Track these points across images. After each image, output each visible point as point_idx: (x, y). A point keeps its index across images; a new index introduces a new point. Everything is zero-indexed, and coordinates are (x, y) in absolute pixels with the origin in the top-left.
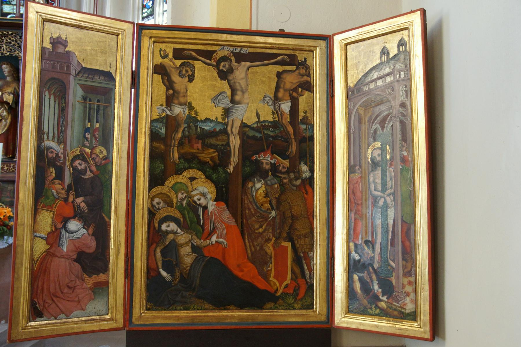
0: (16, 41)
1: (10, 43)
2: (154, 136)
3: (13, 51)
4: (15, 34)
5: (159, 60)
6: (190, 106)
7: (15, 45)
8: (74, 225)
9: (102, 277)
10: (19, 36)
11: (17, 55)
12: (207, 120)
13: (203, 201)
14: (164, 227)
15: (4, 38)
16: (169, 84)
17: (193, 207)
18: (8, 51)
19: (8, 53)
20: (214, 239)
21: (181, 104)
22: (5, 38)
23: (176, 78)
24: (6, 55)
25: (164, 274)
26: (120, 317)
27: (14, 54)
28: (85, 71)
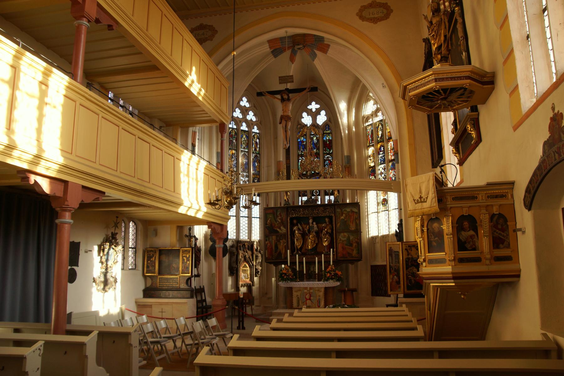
2: (406, 261)
5: (406, 248)
6: (412, 256)
8: (395, 277)
9: (399, 285)
12: (415, 258)
13: (415, 272)
14: (409, 277)
16: (408, 252)
17: (413, 273)
20: (418, 278)
21: (410, 255)
23: (409, 251)
25: (410, 284)
26: (403, 291)
28: (395, 252)
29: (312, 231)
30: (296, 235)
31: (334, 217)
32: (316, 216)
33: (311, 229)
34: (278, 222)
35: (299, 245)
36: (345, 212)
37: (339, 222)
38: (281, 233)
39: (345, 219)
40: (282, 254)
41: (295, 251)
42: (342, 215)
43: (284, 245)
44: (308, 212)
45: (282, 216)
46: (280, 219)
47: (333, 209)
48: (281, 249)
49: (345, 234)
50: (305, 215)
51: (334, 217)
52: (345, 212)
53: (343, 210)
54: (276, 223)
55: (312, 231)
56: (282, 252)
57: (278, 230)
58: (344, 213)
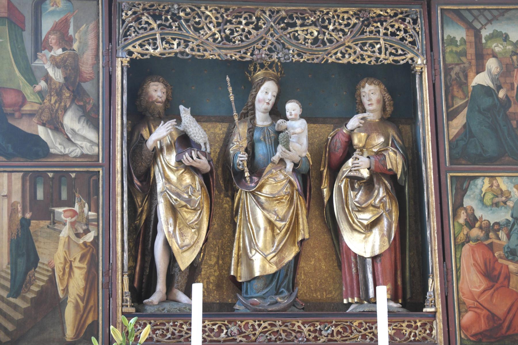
0: (406, 31)
1: (393, 34)
3: (400, 52)
4: (402, 13)
7: (406, 40)
10: (413, 19)
11: (410, 62)
15: (379, 24)
18: (391, 54)
19: (392, 58)
22: (382, 25)
24: (386, 62)
27: (403, 60)
29: (276, 158)
30: (168, 180)
31: (425, 75)
32: (305, 57)
33: (261, 150)
34: (43, 84)
35: (190, 247)
36: (498, 47)
37: (463, 107)
38: (64, 155)
39: (499, 88)
40: (63, 303)
41: (151, 290)
42: (480, 69)
43: (81, 241)
44: (254, 32)
45: (75, 46)
46: (57, 63)
47: (415, 22)
48: (58, 264)
49: (504, 184)
50: (238, 49)
51: (425, 75)
52: (498, 47)
53: (485, 33)
54: (28, 91)
55: (276, 158)
56: (66, 290)
57: (42, 132)
58: (494, 55)
